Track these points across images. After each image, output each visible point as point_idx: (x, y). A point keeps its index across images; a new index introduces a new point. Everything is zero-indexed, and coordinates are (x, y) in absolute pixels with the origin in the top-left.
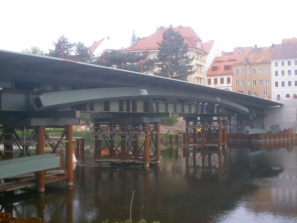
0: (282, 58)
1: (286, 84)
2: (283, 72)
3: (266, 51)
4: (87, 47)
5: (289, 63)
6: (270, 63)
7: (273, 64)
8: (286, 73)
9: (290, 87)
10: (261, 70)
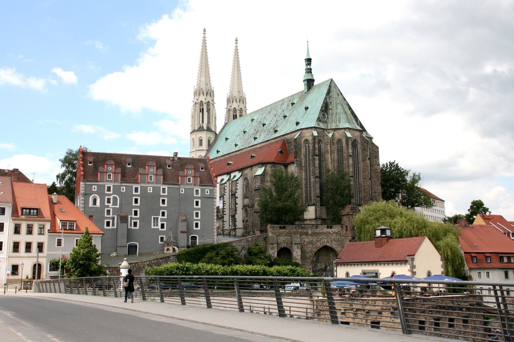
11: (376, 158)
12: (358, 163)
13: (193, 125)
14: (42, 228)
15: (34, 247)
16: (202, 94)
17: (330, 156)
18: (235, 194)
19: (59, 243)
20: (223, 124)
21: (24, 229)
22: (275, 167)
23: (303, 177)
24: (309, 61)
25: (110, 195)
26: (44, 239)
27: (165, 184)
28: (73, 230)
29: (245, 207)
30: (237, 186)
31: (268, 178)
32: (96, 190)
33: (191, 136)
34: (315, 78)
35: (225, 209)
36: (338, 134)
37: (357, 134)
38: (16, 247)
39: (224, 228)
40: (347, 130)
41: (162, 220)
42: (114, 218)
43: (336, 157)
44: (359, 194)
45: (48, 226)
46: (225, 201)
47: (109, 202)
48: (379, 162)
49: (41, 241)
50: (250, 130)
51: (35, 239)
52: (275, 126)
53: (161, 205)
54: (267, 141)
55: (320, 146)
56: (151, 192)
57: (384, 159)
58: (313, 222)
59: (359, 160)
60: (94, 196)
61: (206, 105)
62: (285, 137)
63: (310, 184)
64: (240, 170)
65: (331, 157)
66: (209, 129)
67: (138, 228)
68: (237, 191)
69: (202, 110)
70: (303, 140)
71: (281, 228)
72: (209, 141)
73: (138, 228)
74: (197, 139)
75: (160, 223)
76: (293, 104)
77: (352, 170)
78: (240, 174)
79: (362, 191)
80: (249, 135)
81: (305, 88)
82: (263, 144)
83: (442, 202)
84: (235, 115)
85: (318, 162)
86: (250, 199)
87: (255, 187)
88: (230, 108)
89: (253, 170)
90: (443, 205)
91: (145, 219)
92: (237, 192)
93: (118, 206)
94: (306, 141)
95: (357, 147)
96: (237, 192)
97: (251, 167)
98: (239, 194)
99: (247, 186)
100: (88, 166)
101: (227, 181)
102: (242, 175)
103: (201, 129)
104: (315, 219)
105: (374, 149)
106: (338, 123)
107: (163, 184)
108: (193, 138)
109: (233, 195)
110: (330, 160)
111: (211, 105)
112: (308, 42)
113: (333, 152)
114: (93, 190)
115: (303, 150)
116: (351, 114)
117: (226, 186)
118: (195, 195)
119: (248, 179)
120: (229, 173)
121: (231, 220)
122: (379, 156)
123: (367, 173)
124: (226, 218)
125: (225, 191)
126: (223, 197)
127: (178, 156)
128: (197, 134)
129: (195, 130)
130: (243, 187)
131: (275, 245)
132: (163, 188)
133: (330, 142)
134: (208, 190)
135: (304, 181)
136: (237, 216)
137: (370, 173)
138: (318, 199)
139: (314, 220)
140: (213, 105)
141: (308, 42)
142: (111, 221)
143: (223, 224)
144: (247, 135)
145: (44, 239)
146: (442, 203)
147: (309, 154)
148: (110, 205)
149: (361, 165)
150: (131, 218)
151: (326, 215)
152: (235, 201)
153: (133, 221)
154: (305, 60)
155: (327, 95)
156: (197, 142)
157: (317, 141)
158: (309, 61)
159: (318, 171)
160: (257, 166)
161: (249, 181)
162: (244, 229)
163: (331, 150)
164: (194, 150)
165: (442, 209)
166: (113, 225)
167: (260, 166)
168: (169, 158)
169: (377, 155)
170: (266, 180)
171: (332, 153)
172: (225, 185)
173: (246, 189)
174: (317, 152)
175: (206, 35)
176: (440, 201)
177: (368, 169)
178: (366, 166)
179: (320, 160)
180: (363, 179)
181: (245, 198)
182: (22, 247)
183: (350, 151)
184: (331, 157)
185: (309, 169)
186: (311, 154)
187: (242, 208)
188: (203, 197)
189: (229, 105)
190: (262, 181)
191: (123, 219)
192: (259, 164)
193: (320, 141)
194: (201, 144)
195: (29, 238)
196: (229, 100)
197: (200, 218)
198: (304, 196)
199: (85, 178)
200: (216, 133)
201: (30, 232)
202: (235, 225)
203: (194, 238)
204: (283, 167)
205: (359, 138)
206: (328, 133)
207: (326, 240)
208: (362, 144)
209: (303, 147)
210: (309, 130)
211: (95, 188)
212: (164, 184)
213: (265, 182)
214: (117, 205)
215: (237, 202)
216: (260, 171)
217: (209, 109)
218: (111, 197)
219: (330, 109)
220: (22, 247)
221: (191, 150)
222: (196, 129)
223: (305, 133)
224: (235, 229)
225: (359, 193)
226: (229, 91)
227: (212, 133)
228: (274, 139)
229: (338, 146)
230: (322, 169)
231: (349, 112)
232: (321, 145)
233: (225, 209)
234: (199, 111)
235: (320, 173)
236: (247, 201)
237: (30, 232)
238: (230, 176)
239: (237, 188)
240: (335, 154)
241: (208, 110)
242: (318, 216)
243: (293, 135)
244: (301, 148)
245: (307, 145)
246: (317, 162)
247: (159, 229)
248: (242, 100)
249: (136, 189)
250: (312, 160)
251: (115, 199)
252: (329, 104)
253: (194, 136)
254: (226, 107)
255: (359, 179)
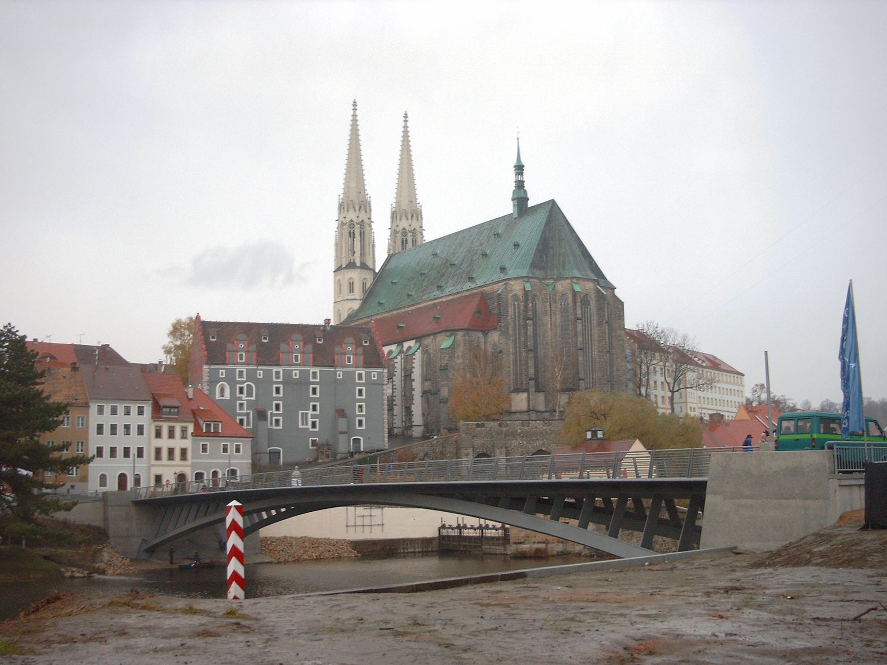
0: (114, 400)
1: (120, 452)
2: (114, 428)
3: (64, 377)
4: (25, 337)
5: (114, 411)
6: (86, 406)
7: (94, 408)
8: (120, 430)
9: (128, 459)
10: (68, 420)
11: (619, 319)
12: (591, 328)
13: (338, 257)
14: (184, 431)
15: (177, 454)
16: (353, 209)
17: (549, 320)
18: (410, 375)
19: (204, 449)
20: (386, 256)
21: (165, 432)
22: (469, 336)
23: (511, 350)
24: (520, 168)
25: (243, 382)
26: (187, 443)
27: (316, 366)
28: (218, 432)
29: (424, 393)
30: (413, 363)
31: (460, 351)
32: (224, 376)
33: (335, 277)
34: (529, 195)
35: (395, 396)
36: (561, 286)
37: (590, 285)
38: (158, 451)
39: (395, 426)
40: (575, 280)
41: (313, 416)
42: (249, 413)
43: (559, 321)
44: (593, 375)
45: (191, 428)
46: (395, 385)
47: (241, 390)
48: (624, 324)
49: (184, 446)
50: (430, 271)
51: (178, 443)
52: (469, 269)
53: (311, 396)
54: (458, 293)
55: (535, 304)
56: (298, 377)
57: (631, 322)
58: (525, 417)
59: (592, 325)
60: (222, 384)
61: (359, 226)
62: (484, 288)
63: (520, 360)
64: (418, 338)
65: (551, 321)
66: (364, 266)
67: (281, 427)
68: (413, 370)
69: (352, 235)
70: (511, 294)
71: (478, 426)
72: (364, 284)
73: (281, 427)
74: (346, 281)
75: (310, 421)
76: (498, 235)
77: (581, 339)
78: (418, 344)
79: (597, 369)
80: (429, 280)
81: (514, 212)
82: (451, 298)
83: (739, 376)
84: (404, 239)
85: (531, 329)
86: (433, 383)
87: (441, 366)
88: (396, 228)
89: (437, 340)
90: (741, 381)
91: (290, 417)
92: (413, 372)
93: (254, 398)
94: (516, 297)
95: (589, 304)
96: (413, 372)
97: (434, 334)
98: (417, 374)
99: (427, 364)
100: (211, 341)
101: (398, 355)
102: (420, 345)
103: (351, 265)
104: (526, 412)
105: (616, 305)
106: (561, 270)
107: (313, 366)
108: (339, 280)
109: (408, 376)
110: (549, 325)
111: (367, 226)
112: (518, 139)
113: (555, 314)
114: (221, 376)
115: (511, 310)
116: (581, 254)
117: (397, 363)
118: (357, 381)
119: (429, 353)
120: (400, 343)
121: (404, 413)
122: (623, 316)
123: (603, 343)
124: (397, 410)
125: (396, 370)
126: (392, 379)
127: (330, 324)
128: (345, 273)
129: (341, 266)
130: (422, 365)
131: (470, 450)
132: (313, 372)
133: (550, 299)
134: (375, 373)
135: (511, 357)
136: (413, 408)
137: (607, 343)
138: (532, 383)
139: (526, 413)
140: (370, 226)
141: (518, 139)
142: (245, 418)
143: (393, 420)
144: (426, 279)
145: (187, 443)
146: (736, 378)
147: (519, 316)
148: (244, 396)
149: (596, 331)
150: (271, 413)
151: (544, 406)
152: (411, 386)
153: (274, 418)
154: (515, 166)
155: (545, 226)
156: (345, 287)
157: (530, 298)
158: (520, 168)
159: (532, 341)
160: (443, 334)
161: (432, 355)
162: (425, 427)
163: (551, 310)
164: (340, 299)
165: (740, 388)
166: (248, 424)
167: (448, 334)
168: (318, 326)
169: (622, 314)
170: (456, 355)
171: (553, 314)
172: (396, 360)
173: (426, 367)
174: (530, 314)
175: (357, 111)
176: (736, 376)
177: (605, 337)
178: (603, 333)
179: (535, 324)
180: (598, 352)
181: (427, 380)
182: (165, 454)
183: (579, 312)
184: (551, 321)
185: (519, 338)
186: (522, 317)
187: (421, 394)
188: (369, 383)
189: (395, 224)
190: (450, 357)
191: (261, 415)
192: (446, 331)
193: (534, 297)
194: (351, 290)
195: (171, 443)
196: (395, 215)
197: (364, 413)
198: (512, 379)
199: (211, 361)
200: (374, 271)
201: (171, 435)
202: (410, 421)
203: (357, 441)
204: (480, 335)
205: (593, 292)
206: (547, 285)
207: (541, 442)
208: (597, 301)
209: (510, 305)
210: (520, 281)
211: (222, 373)
212: (314, 365)
213: (454, 357)
214: (252, 397)
215: (413, 387)
216: (447, 343)
217: (364, 233)
218: (245, 385)
219: (551, 248)
220: (165, 454)
221: (335, 299)
222: (344, 266)
223: (513, 285)
224: (412, 426)
225: (592, 373)
226: (394, 200)
227: (369, 271)
228: (467, 290)
229: (561, 304)
230: (538, 338)
231: (578, 252)
232: (537, 303)
233: (395, 396)
234: (347, 234)
235: (535, 344)
236: (427, 384)
237: (171, 435)
238: (402, 347)
239: (414, 365)
240: (558, 316)
241: (362, 234)
242: (531, 407)
243: (496, 286)
244: (507, 307)
245: (516, 303)
246: (530, 329)
247: (309, 428)
248: (416, 214)
249: (278, 373)
250: (523, 325)
251: (249, 388)
252: (550, 239)
253: (340, 277)
254: (390, 227)
255: (592, 353)
